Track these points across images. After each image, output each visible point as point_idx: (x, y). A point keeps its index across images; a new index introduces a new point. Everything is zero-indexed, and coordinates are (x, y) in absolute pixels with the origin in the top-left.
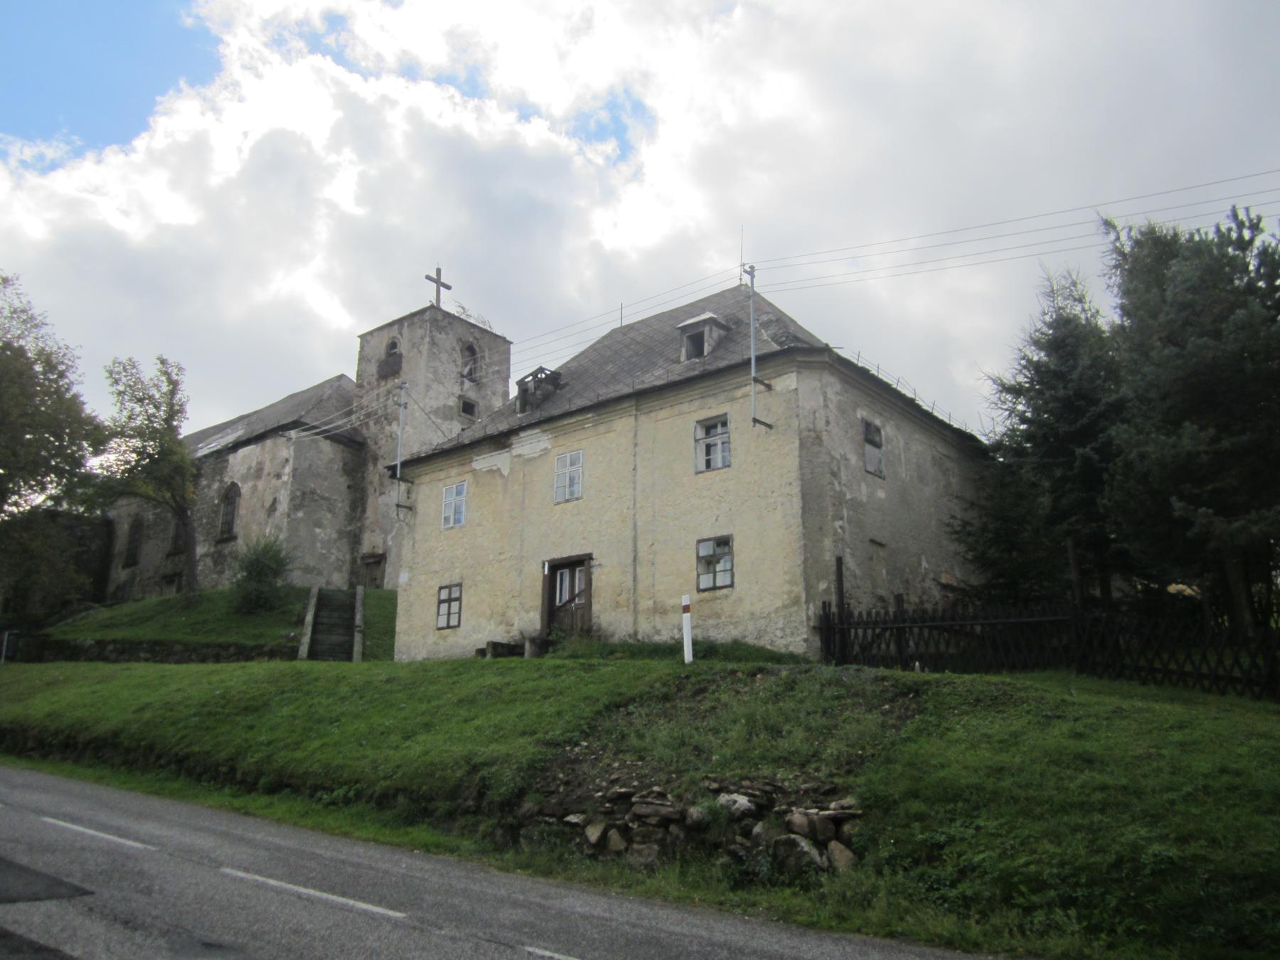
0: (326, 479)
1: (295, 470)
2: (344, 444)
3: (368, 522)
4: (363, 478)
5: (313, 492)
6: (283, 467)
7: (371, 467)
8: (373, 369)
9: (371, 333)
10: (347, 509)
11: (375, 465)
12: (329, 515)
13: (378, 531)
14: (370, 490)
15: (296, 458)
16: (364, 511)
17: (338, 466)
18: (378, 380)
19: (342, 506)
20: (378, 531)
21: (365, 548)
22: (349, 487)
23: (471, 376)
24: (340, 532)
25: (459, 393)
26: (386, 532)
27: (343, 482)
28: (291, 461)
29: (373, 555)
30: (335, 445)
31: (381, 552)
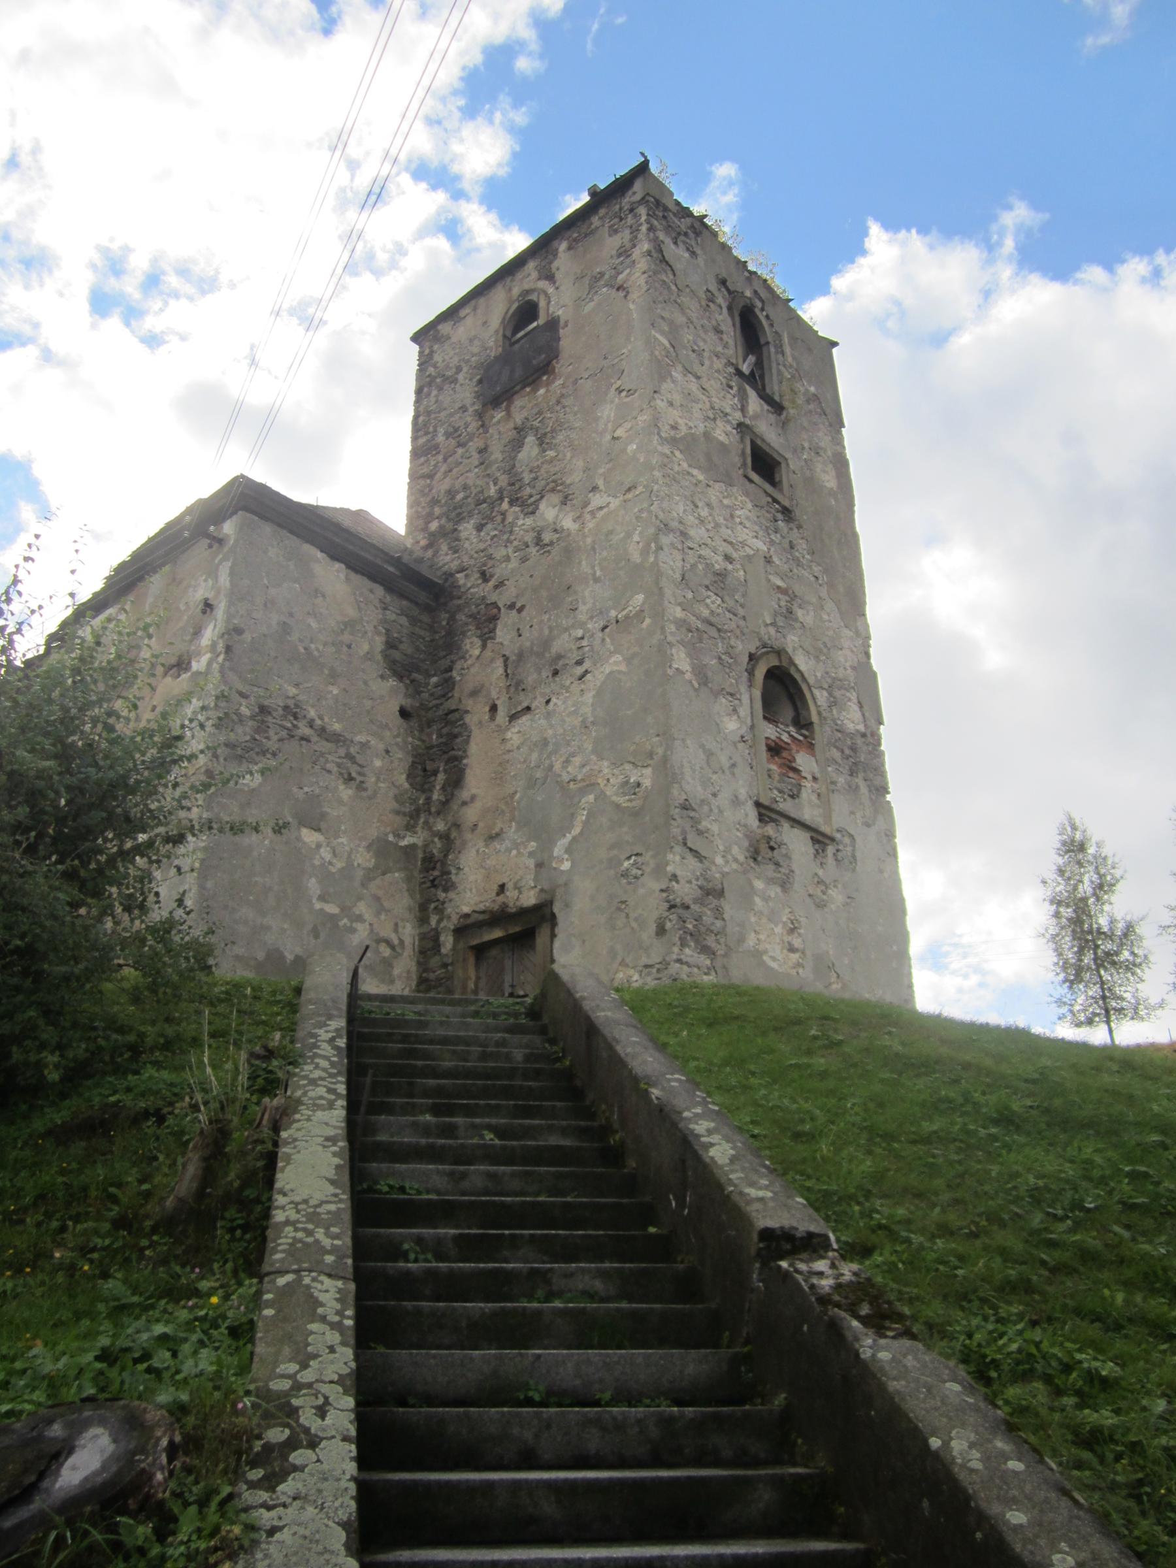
0: (333, 676)
1: (233, 631)
2: (390, 588)
3: (470, 814)
4: (448, 684)
5: (293, 712)
6: (197, 633)
7: (472, 646)
8: (465, 393)
9: (451, 314)
10: (402, 780)
11: (487, 637)
12: (346, 793)
13: (512, 832)
14: (477, 713)
15: (236, 596)
16: (456, 780)
17: (370, 643)
18: (480, 415)
19: (386, 758)
20: (512, 832)
21: (471, 894)
22: (404, 713)
23: (756, 379)
24: (381, 848)
25: (737, 416)
26: (543, 834)
27: (388, 695)
28: (220, 612)
29: (498, 917)
30: (357, 579)
31: (529, 899)
